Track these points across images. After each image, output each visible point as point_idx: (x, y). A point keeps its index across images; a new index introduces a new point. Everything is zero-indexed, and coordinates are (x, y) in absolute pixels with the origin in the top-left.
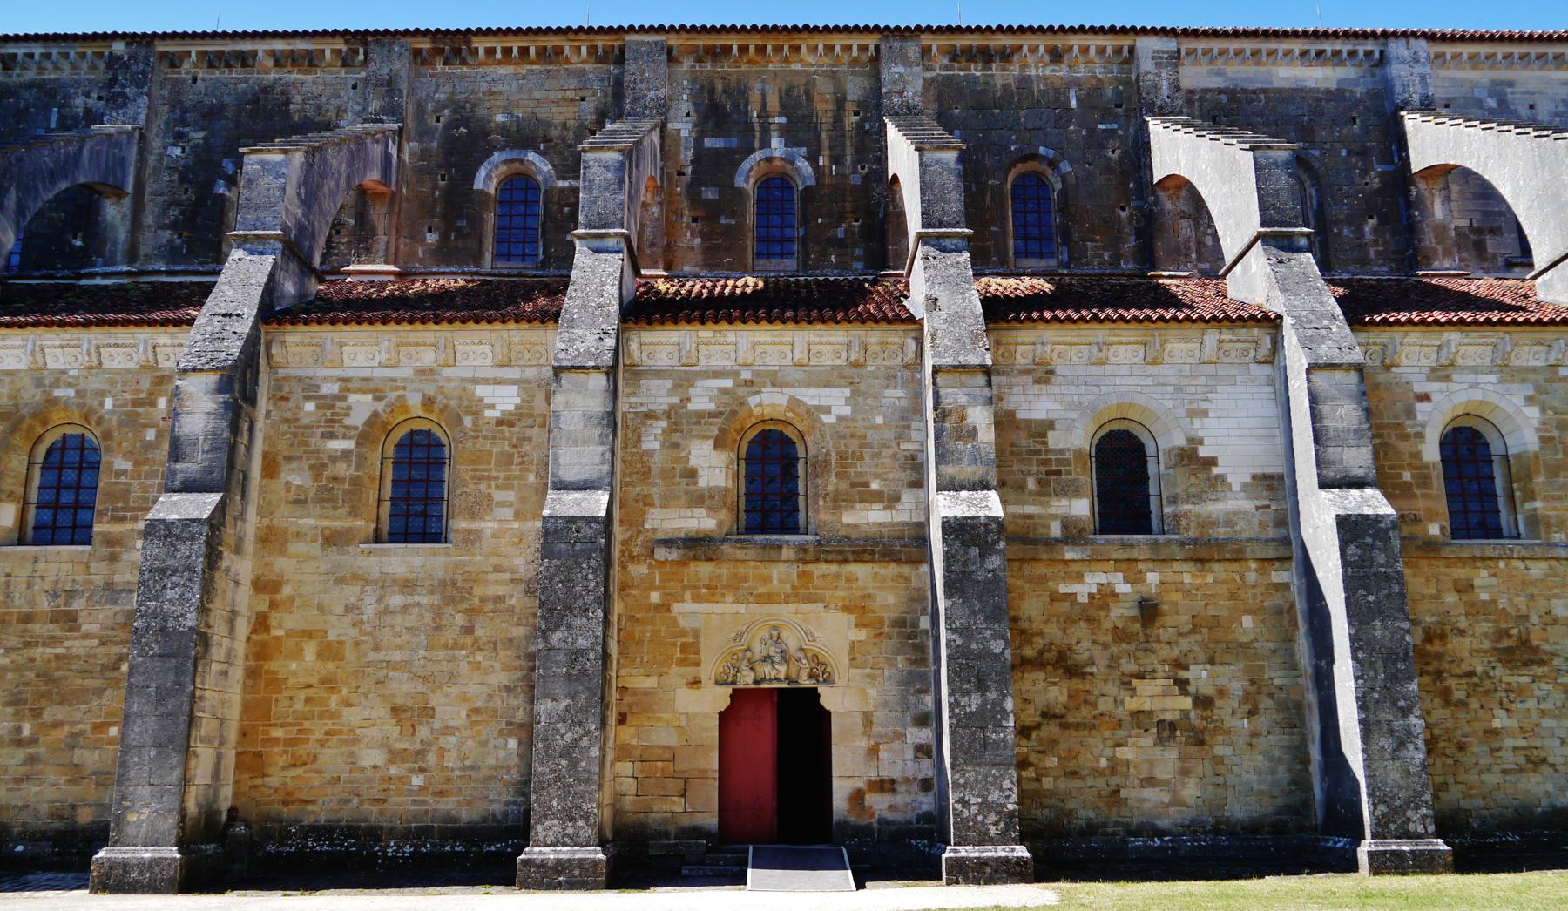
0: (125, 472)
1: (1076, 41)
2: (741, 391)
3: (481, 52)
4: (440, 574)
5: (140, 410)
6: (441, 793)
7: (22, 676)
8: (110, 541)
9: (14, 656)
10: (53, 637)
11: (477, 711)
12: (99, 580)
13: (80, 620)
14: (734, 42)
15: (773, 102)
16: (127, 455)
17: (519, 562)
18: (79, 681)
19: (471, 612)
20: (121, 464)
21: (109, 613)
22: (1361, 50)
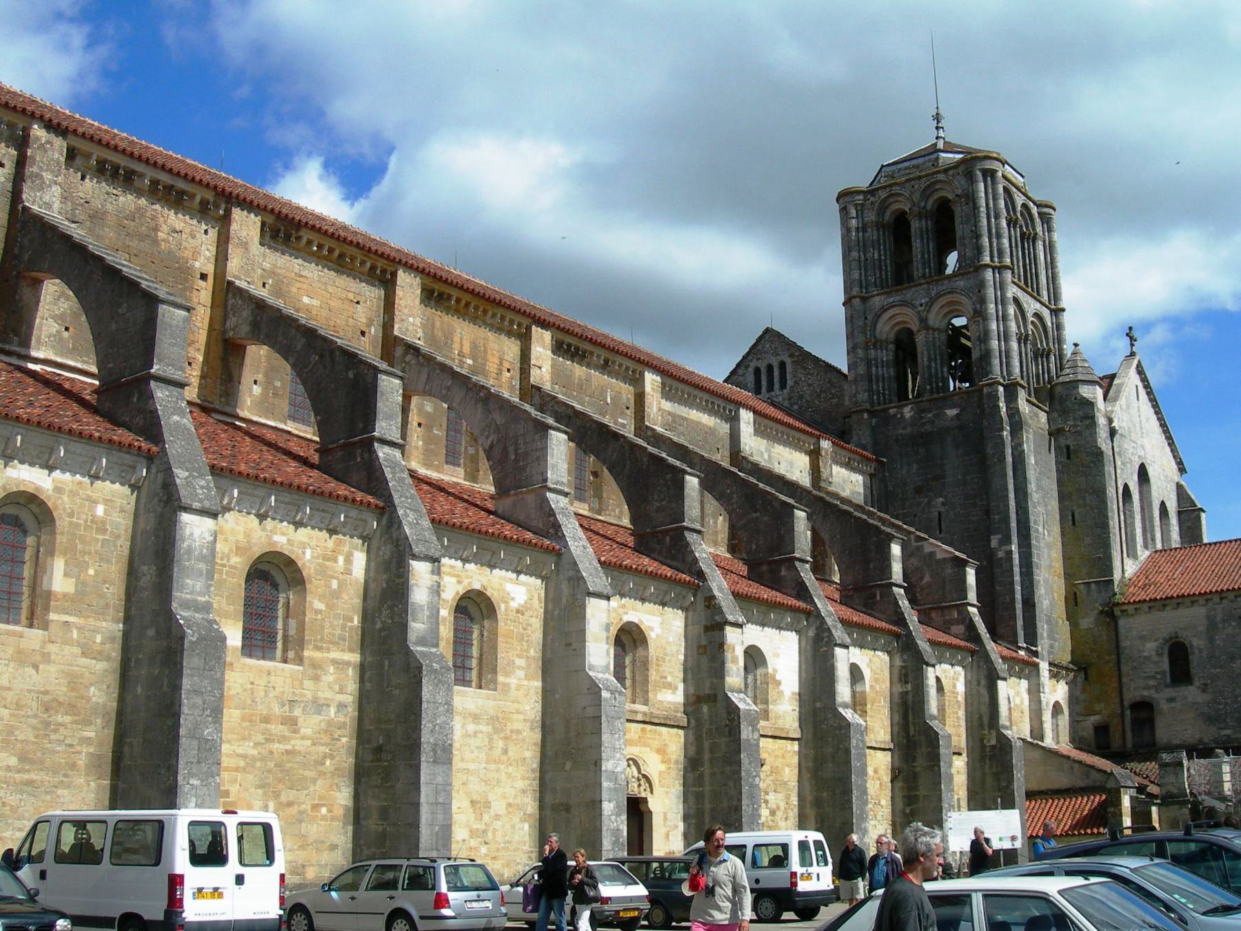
0: (320, 611)
1: (619, 359)
2: (621, 611)
3: (304, 241)
4: (492, 713)
5: (328, 563)
6: (494, 858)
7: (266, 765)
8: (315, 665)
9: (259, 749)
10: (283, 737)
11: (509, 805)
12: (309, 695)
13: (299, 725)
14: (455, 294)
15: (466, 350)
16: (322, 598)
17: (527, 707)
18: (301, 772)
19: (506, 738)
20: (319, 605)
21: (317, 721)
22: (728, 407)
